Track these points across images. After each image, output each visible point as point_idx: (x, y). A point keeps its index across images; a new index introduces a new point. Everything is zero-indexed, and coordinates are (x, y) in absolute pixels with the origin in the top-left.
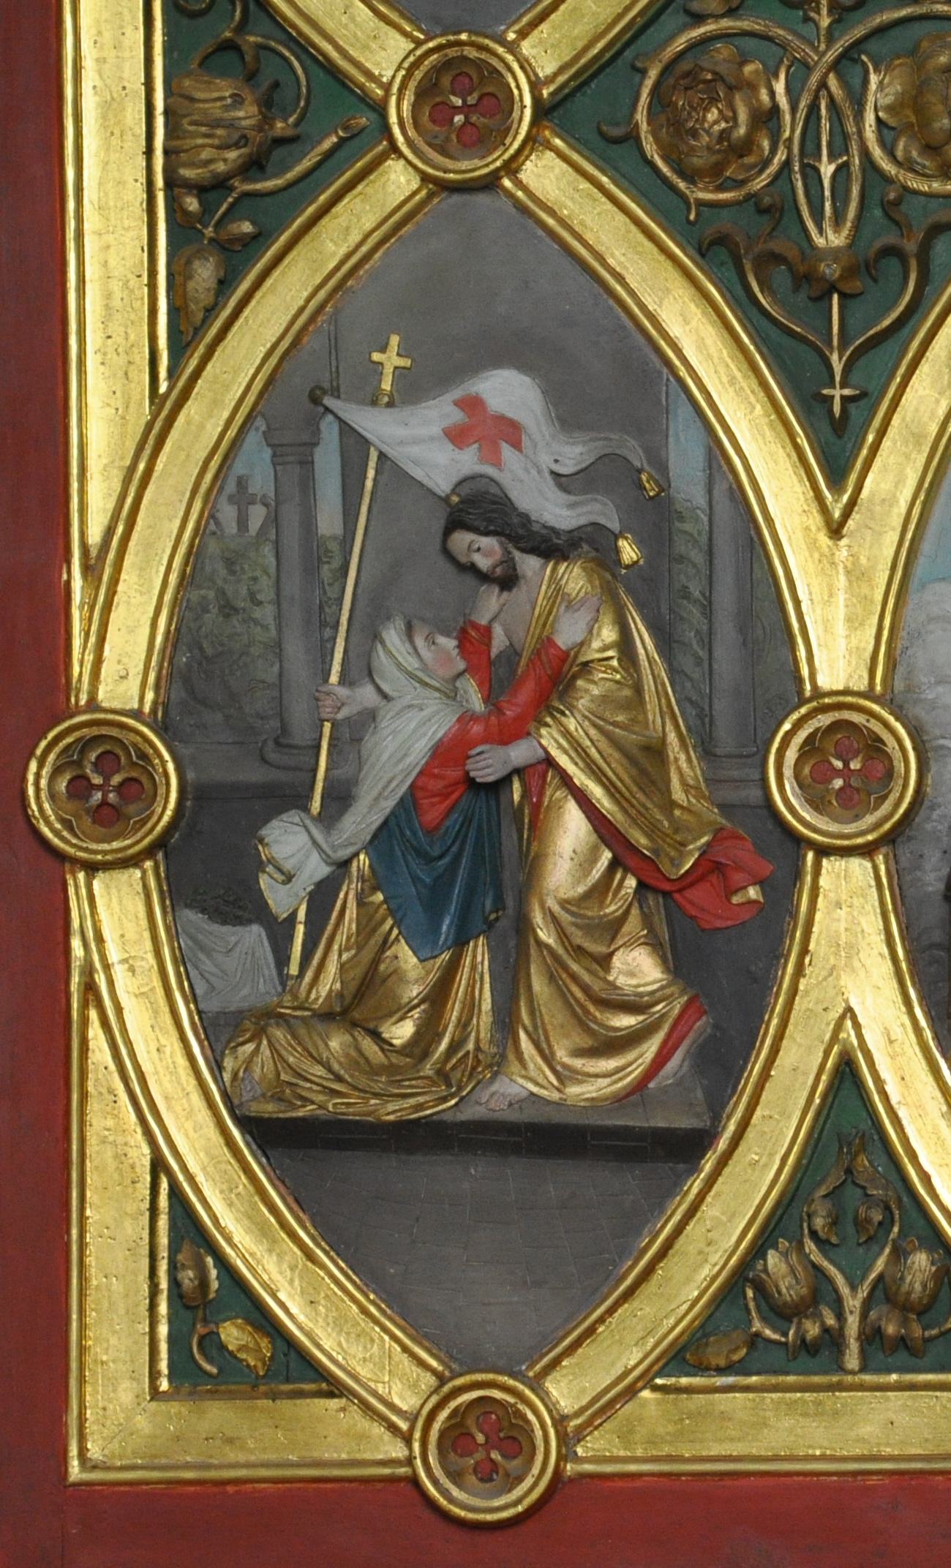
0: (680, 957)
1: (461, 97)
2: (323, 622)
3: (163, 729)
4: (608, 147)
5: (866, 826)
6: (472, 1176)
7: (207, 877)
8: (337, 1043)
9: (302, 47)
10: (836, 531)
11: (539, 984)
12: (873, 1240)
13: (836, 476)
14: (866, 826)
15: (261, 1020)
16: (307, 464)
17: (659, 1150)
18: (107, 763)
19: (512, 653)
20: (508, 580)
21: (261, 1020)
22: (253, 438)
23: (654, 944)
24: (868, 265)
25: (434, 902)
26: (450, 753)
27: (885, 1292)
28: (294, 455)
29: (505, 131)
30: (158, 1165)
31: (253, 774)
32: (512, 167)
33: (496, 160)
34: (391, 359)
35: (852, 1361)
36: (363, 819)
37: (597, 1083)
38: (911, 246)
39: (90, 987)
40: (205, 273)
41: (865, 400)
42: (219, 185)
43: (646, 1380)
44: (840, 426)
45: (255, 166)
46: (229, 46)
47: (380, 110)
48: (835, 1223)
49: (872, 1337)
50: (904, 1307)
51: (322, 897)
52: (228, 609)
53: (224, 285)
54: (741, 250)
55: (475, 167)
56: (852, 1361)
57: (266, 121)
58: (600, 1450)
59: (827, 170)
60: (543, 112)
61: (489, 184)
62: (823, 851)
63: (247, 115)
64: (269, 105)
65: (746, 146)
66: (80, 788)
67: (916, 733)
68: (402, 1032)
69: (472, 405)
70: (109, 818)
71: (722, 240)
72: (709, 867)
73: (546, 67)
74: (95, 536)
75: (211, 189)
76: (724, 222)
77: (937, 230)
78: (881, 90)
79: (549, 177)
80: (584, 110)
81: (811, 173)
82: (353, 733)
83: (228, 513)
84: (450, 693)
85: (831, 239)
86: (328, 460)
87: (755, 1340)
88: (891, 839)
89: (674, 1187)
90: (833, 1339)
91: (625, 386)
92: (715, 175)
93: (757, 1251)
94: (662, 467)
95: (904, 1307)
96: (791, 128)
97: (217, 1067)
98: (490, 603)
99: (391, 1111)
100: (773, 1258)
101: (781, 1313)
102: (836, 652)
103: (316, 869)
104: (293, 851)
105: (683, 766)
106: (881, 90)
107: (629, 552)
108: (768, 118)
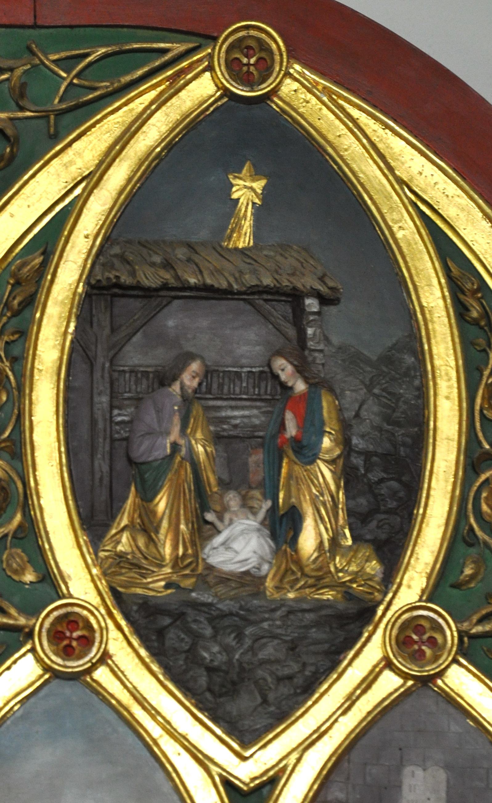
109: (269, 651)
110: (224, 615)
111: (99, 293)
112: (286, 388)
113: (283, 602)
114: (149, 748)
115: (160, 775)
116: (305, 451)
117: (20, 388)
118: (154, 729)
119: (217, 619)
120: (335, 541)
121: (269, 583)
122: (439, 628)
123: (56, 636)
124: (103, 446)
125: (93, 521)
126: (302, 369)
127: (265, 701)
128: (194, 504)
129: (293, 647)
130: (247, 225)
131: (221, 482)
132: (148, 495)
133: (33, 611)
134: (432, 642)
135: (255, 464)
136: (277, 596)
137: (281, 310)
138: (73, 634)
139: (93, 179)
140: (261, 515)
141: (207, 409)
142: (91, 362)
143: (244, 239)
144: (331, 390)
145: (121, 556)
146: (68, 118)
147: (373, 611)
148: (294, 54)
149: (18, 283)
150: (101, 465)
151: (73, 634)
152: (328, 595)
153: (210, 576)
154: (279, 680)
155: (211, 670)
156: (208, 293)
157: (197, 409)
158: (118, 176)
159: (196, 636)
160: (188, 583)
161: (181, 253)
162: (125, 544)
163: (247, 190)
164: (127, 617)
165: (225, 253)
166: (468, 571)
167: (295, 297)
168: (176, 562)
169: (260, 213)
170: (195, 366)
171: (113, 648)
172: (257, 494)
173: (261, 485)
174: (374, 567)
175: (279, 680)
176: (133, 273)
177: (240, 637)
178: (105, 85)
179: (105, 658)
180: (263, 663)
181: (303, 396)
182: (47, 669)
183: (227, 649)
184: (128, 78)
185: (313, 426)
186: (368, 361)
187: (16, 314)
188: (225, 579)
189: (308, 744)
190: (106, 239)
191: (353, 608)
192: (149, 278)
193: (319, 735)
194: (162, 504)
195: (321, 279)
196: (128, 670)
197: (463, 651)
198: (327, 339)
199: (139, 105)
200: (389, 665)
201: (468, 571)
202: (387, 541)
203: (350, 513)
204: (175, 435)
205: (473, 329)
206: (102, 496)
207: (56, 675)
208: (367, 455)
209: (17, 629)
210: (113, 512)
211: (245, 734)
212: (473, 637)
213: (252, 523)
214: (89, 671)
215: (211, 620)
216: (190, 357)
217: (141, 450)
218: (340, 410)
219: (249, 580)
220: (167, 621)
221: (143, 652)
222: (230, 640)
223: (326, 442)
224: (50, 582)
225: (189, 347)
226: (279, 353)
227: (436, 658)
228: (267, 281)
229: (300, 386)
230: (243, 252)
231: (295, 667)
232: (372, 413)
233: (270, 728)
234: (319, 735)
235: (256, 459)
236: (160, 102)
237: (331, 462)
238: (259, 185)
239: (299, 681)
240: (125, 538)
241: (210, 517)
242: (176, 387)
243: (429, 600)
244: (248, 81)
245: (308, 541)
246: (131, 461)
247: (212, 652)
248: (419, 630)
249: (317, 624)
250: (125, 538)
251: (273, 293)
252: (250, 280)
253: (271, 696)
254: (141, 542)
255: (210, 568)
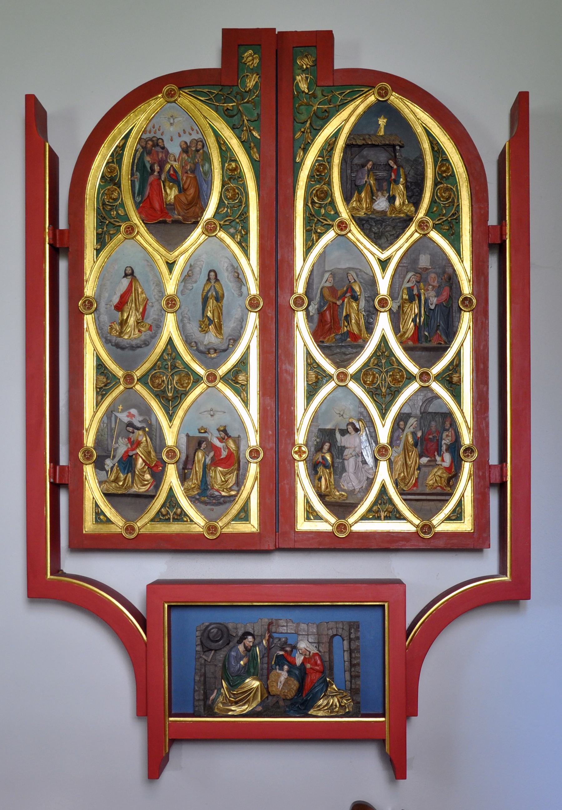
0: (152, 475)
1: (129, 378)
2: (112, 437)
3: (94, 449)
4: (145, 384)
5: (173, 461)
6: (129, 500)
7: (99, 465)
8: (113, 484)
9: (111, 373)
10: (170, 427)
11: (136, 478)
12: (174, 507)
13: (170, 421)
14: (173, 461)
15: (105, 482)
16: (111, 419)
17: (150, 497)
18: (88, 453)
19: (134, 441)
20: (133, 433)
21: (105, 482)
22: (105, 416)
23: (149, 474)
24: (174, 398)
25: (125, 469)
26: (126, 452)
27: (175, 513)
28: (109, 418)
29: (133, 382)
30: (93, 498)
31: (105, 454)
32: (134, 386)
33: (132, 385)
34: (120, 408)
35: (171, 521)
36: (117, 459)
37: (143, 489)
38: (179, 396)
39: (86, 478)
40: (100, 398)
41: (174, 413)
42: (102, 388)
43: (148, 523)
44: (171, 416)
45: (105, 386)
46: (103, 372)
47: (119, 379)
48: (170, 505)
49: (174, 518)
50: (177, 515)
51: (112, 468)
52: (102, 435)
53: (102, 399)
54: (160, 396)
55: (131, 386)
56: (171, 521)
57: (107, 381)
58: (143, 531)
59: (170, 387)
60: (138, 380)
61: (132, 388)
62: (168, 464)
63: (105, 380)
64: (107, 379)
65: (161, 384)
66: (85, 455)
67: (179, 451)
68: (121, 483)
69: (130, 413)
70: (88, 459)
71: (158, 395)
72: (156, 465)
73: (138, 375)
74: (87, 427)
75: (100, 388)
76: (158, 393)
77: (182, 394)
78: (176, 378)
79: (139, 387)
80: (142, 380)
81: (168, 387)
82: (115, 450)
83: (102, 425)
84: (127, 445)
85: (170, 395)
86: (113, 419)
87: (160, 519)
88: (176, 462)
89: (151, 501)
90: (169, 519)
91: (147, 411)
92: (157, 387)
93: (161, 509)
94: (151, 420)
95: (177, 515)
96: (166, 382)
97: (100, 487)
98: (131, 435)
99: (120, 492)
100: (162, 509)
101: (163, 516)
102: (170, 440)
103: (111, 465)
104: (109, 463)
105: (153, 454)
106: (176, 378)
107: (147, 429)
108: (163, 381)
109: (388, 229)
110: (378, 221)
111: (348, 146)
112: (391, 167)
113: (392, 217)
114: (360, 251)
115: (363, 258)
116: (396, 182)
117: (330, 169)
118: (362, 247)
119: (376, 221)
120: (404, 203)
121: (388, 213)
122: (428, 222)
123: (339, 226)
124: (349, 182)
125: (347, 199)
126: (396, 163)
127: (387, 240)
128: (370, 195)
129: (394, 227)
130: (382, 130)
131: (377, 190)
132: (360, 193)
133: (333, 220)
134: (426, 226)
135: (385, 184)
136: (390, 216)
137: (390, 149)
138: (343, 226)
139: (347, 120)
140: (386, 197)
141: (373, 173)
142: (346, 162)
143: (382, 133)
144: (402, 167)
145: (354, 207)
146: (341, 107)
147: (413, 219)
148: (393, 90)
149: (329, 145)
150: (349, 186)
151: (343, 226)
152: (402, 215)
153: (374, 212)
154: (391, 235)
155: (375, 233)
156: (373, 146)
157: (371, 173)
158: (352, 119)
159: (371, 226)
160: (369, 213)
161: (367, 137)
162: (354, 204)
163: (382, 122)
164: (355, 221)
165: (377, 136)
166: (435, 209)
167: (394, 146)
168: (366, 209)
169: (385, 127)
170: (371, 163)
171: (352, 229)
172: (385, 192)
173: (386, 190)
174: (413, 209)
175: (391, 235)
176: (356, 142)
177: (381, 226)
178: (349, 99)
179: (350, 231)
180: (387, 231)
181: (396, 169)
182: (337, 234)
183: (379, 229)
184: (354, 97)
185: (398, 176)
186: (411, 161)
187: (329, 152)
188: (378, 212)
189: (398, 250)
190: (350, 134)
191: (408, 218)
192: (360, 142)
193: (400, 248)
194: (363, 195)
195: (400, 142)
196: (355, 234)
197: (434, 228)
198: (402, 156)
199: (357, 103)
200: (416, 231)
201: (435, 209)
202: (416, 203)
203: (407, 196)
204: (366, 179)
205: (436, 153)
206: (350, 194)
207: (339, 235)
208: (411, 183)
209: (329, 225)
210: (351, 197)
211: (383, 248)
212: (436, 224)
213: (384, 199)
214: (346, 234)
215: (375, 222)
216: (369, 161)
217: (358, 183)
218: (405, 172)
219: (384, 212)
220: (364, 222)
221: (359, 229)
222: (379, 226)
223: (401, 180)
224: (337, 214)
225: (369, 158)
226: (390, 159)
227: (427, 229)
228: (387, 143)
229: (395, 167)
230: (382, 136)
231: (395, 232)
232: (412, 173)
233: (389, 246)
234: (400, 248)
235: (385, 184)
236: (362, 102)
237: (403, 184)
238: (385, 120)
239: (395, 235)
240: (354, 203)
241: (374, 198)
242: (366, 168)
243: (426, 216)
244: (382, 96)
245: (397, 203)
246: (355, 185)
247: (375, 229)
248: (424, 223)
249: (400, 222)
250: (354, 203)
251: (389, 145)
252: (383, 142)
253: (389, 239)
254: (358, 204)
255: (374, 210)
